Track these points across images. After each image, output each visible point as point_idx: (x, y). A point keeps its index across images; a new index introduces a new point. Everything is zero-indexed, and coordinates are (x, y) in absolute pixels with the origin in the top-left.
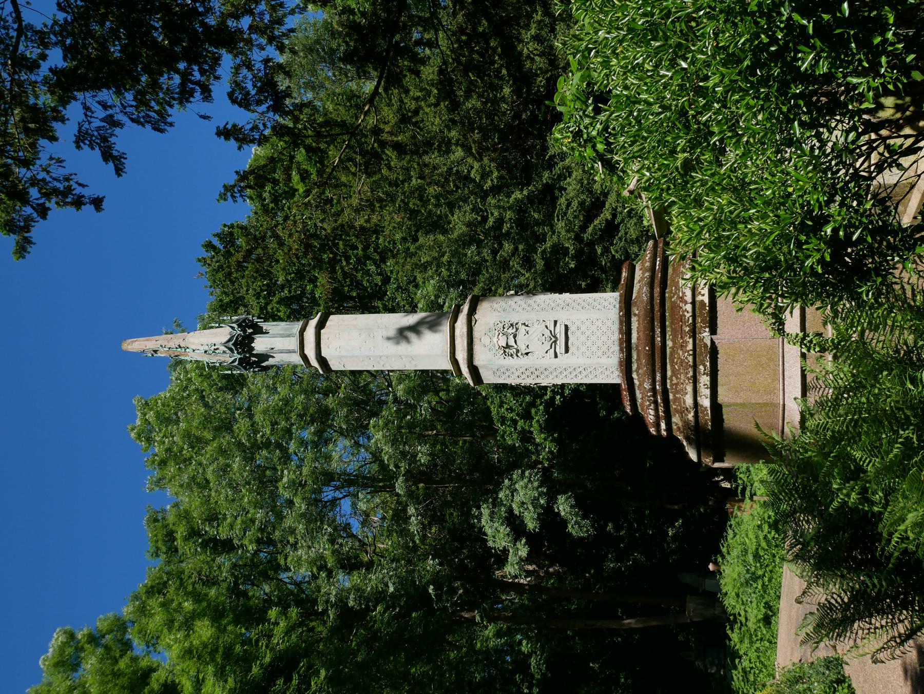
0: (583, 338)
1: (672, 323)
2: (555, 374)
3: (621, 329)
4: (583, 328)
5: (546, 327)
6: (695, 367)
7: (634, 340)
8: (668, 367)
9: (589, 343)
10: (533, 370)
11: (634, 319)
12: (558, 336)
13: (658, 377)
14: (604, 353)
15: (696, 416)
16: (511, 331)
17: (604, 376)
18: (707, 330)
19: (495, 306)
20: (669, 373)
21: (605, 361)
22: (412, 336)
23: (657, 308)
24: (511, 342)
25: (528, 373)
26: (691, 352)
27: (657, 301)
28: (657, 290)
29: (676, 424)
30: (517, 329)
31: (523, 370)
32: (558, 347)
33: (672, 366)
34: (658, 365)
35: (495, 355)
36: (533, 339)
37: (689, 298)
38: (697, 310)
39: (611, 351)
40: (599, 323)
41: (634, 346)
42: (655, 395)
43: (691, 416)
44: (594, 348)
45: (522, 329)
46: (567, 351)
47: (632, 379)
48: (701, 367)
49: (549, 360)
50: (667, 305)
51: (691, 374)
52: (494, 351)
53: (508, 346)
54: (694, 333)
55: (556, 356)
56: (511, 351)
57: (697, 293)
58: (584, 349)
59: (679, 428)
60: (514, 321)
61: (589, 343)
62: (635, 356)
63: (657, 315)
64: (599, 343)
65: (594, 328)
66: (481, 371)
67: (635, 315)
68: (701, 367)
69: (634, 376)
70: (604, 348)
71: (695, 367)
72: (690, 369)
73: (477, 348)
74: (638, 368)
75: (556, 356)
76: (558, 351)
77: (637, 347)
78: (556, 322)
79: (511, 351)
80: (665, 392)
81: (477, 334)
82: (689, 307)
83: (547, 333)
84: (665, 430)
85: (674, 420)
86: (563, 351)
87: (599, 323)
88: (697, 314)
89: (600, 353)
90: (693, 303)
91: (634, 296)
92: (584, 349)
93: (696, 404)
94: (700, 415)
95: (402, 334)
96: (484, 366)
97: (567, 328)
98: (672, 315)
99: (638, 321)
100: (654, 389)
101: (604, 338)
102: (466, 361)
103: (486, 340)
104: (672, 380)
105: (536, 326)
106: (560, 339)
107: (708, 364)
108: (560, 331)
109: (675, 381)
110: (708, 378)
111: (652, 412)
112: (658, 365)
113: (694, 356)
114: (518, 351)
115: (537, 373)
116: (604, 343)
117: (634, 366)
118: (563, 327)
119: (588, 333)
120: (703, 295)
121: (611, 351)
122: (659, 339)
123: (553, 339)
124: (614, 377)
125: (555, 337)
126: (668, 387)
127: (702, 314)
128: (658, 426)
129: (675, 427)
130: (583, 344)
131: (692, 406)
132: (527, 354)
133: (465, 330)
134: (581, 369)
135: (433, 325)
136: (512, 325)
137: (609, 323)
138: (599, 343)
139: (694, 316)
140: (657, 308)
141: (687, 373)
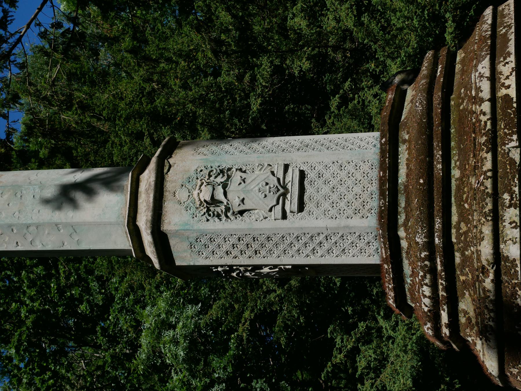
0: (326, 190)
1: (460, 142)
2: (281, 247)
3: (382, 164)
4: (327, 175)
5: (273, 173)
6: (496, 196)
7: (402, 178)
8: (454, 209)
9: (335, 197)
10: (248, 239)
11: (403, 149)
12: (289, 186)
13: (438, 225)
14: (356, 212)
15: (497, 281)
16: (220, 179)
17: (355, 251)
18: (515, 137)
19: (202, 150)
20: (455, 218)
21: (356, 222)
22: (79, 196)
23: (437, 121)
24: (219, 195)
25: (241, 246)
26: (489, 174)
27: (437, 110)
28: (437, 95)
29: (466, 313)
30: (229, 177)
31: (233, 240)
32: (288, 203)
33: (460, 206)
34: (437, 205)
35: (194, 216)
36: (252, 190)
37: (486, 93)
38: (499, 111)
39: (367, 207)
40: (351, 168)
41: (401, 187)
42: (431, 258)
43: (488, 283)
44: (342, 204)
45: (237, 177)
46: (301, 207)
47: (398, 239)
48: (506, 196)
49: (273, 224)
50: (453, 116)
51: (490, 206)
52: (193, 210)
53: (214, 201)
54: (493, 145)
55: (284, 216)
56: (218, 209)
57: (498, 85)
58: (326, 205)
59: (469, 319)
60: (225, 165)
61: (335, 197)
62: (402, 203)
63: (438, 130)
64: (350, 197)
65: (343, 174)
66: (173, 242)
67: (404, 141)
68: (506, 196)
69: (402, 233)
70: (357, 204)
71: (496, 196)
72: (489, 200)
73: (169, 207)
74: (407, 220)
75: (284, 216)
76: (287, 208)
77: (406, 187)
78: (286, 167)
79: (218, 209)
80: (448, 250)
81: (169, 185)
82: (486, 107)
83: (273, 181)
84: (448, 326)
85: (462, 306)
86: (295, 208)
87: (351, 168)
88: (499, 117)
89: (350, 212)
90: (493, 100)
91: (403, 117)
92: (326, 205)
93: (498, 256)
94: (505, 278)
95: (66, 196)
96: (177, 233)
97: (302, 175)
98: (461, 134)
99: (409, 149)
100: (430, 245)
101: (357, 189)
102: (149, 225)
103: (182, 195)
104: (458, 228)
105: (257, 172)
106: (293, 192)
107: (516, 189)
108: (293, 177)
109: (464, 227)
110: (517, 211)
111: (427, 290)
112: (437, 205)
113: (495, 179)
114: (228, 209)
115: (255, 246)
116: (357, 196)
117: (402, 219)
118: (297, 173)
119: (334, 182)
120: (509, 87)
121: (367, 207)
122: (440, 166)
123: (282, 191)
124: (371, 254)
125: (284, 187)
126: (454, 240)
127: (506, 115)
128: (435, 318)
129: (463, 320)
130: (326, 197)
131: (490, 258)
132: (241, 213)
133: (153, 179)
134: (322, 237)
135: (109, 183)
136: (222, 171)
137: (366, 167)
138: (350, 197)
139: (494, 119)
140: (437, 121)
141: (483, 207)
